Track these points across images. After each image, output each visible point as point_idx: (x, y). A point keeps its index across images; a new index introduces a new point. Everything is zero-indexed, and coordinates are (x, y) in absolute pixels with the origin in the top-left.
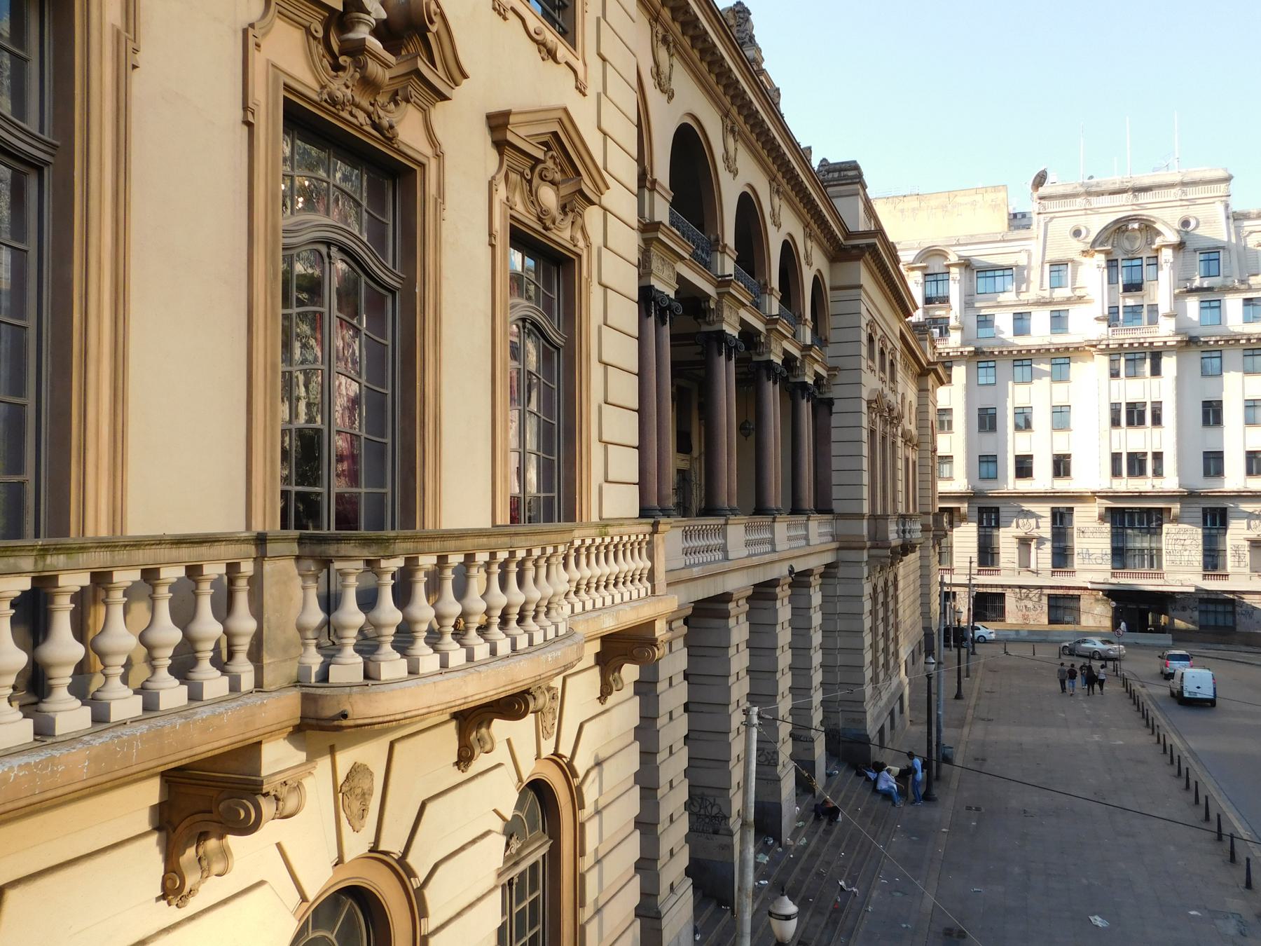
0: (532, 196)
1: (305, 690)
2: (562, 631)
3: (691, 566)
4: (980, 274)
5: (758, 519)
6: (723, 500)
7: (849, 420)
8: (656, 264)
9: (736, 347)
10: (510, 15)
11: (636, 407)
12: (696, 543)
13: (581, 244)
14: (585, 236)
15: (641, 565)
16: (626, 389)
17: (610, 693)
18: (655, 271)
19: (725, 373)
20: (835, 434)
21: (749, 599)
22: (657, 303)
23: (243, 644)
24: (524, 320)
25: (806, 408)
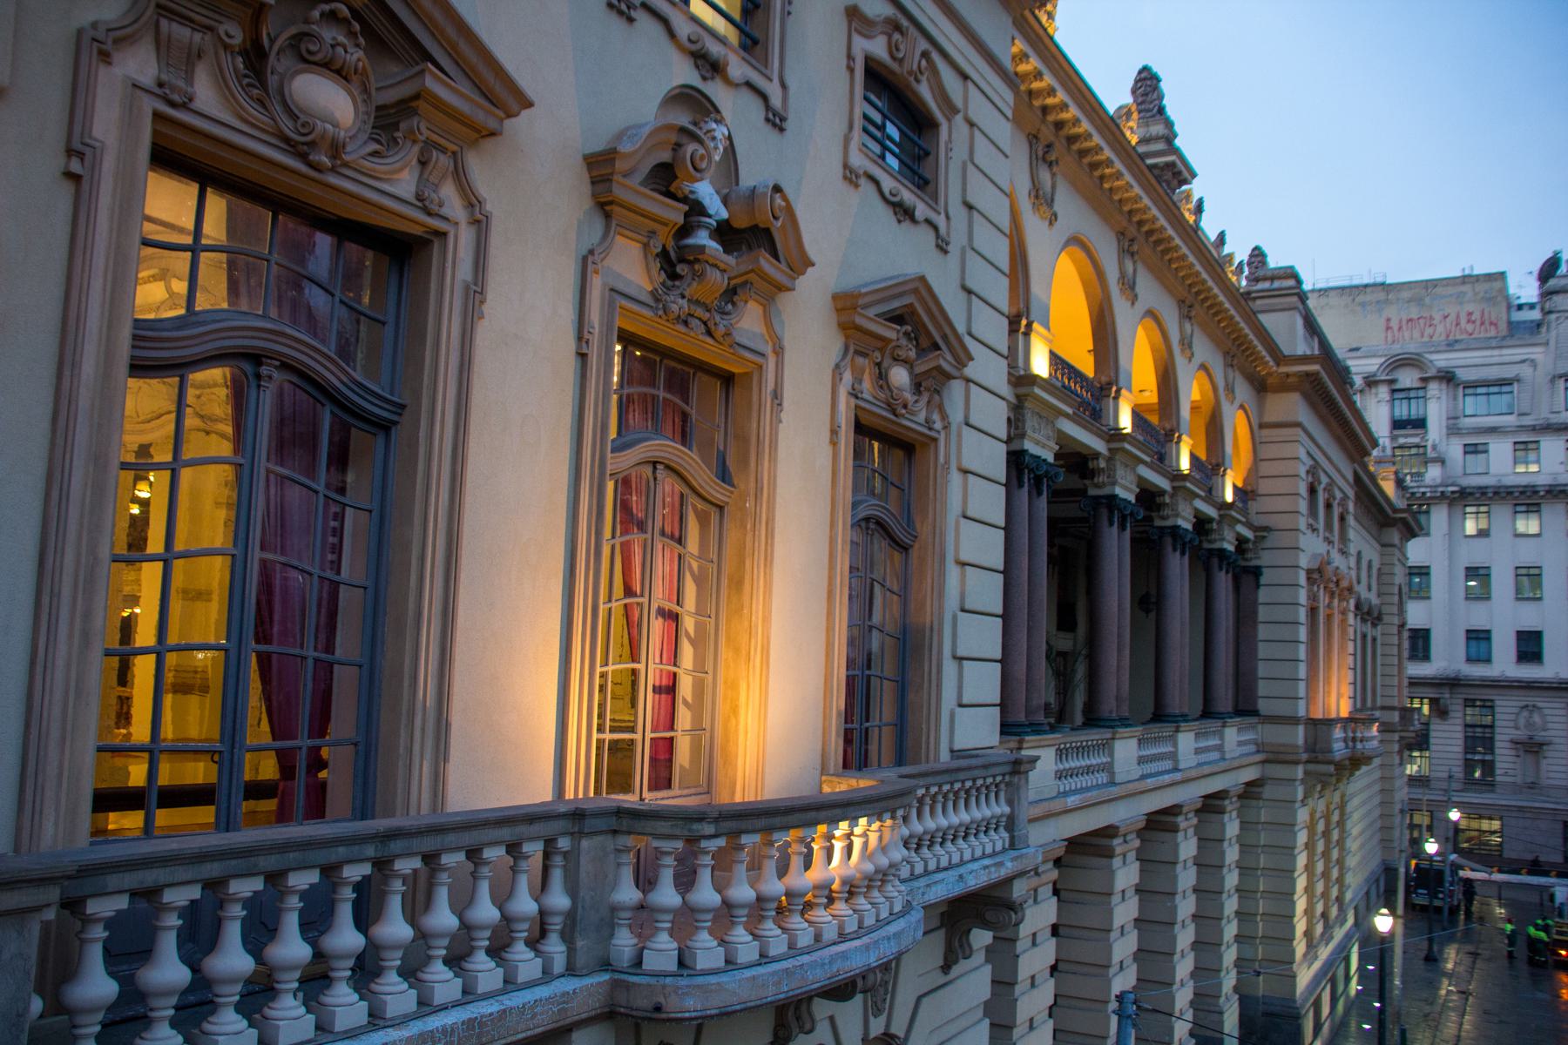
0: (882, 377)
1: (617, 976)
2: (897, 908)
3: (1066, 794)
4: (1469, 391)
5: (1156, 729)
6: (1108, 706)
7: (1284, 595)
8: (1030, 423)
9: (1131, 514)
10: (863, 181)
11: (1000, 611)
12: (1073, 763)
13: (938, 425)
14: (944, 417)
15: (998, 810)
16: (988, 592)
17: (956, 962)
18: (1029, 432)
19: (1116, 548)
20: (1263, 613)
21: (1140, 833)
22: (1031, 471)
23: (556, 923)
24: (867, 519)
25: (1223, 581)
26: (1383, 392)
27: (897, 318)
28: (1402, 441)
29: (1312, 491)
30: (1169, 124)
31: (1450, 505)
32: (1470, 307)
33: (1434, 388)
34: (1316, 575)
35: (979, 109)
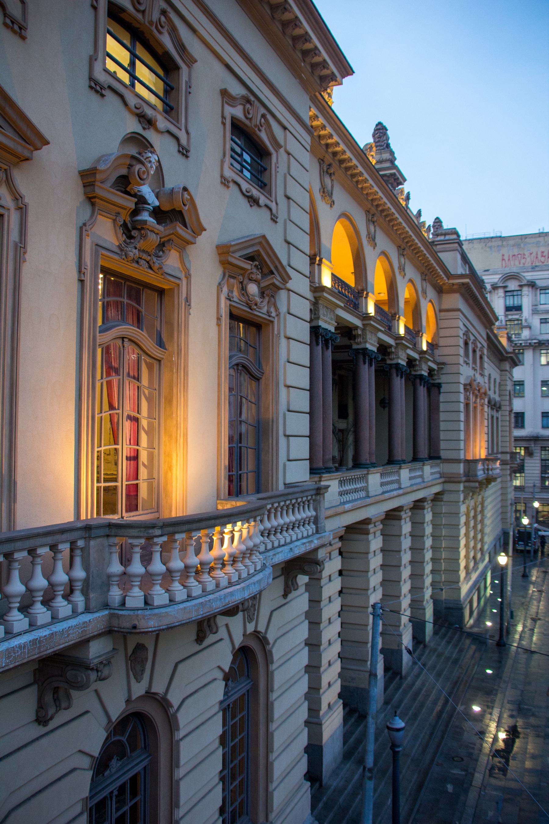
0: (243, 289)
1: (112, 611)
2: (258, 568)
3: (344, 503)
4: (542, 292)
5: (389, 468)
6: (365, 457)
7: (452, 397)
8: (322, 311)
9: (375, 358)
10: (231, 184)
11: (308, 410)
12: (348, 487)
13: (274, 314)
14: (277, 309)
15: (309, 514)
16: (302, 401)
17: (290, 592)
18: (321, 316)
19: (367, 375)
20: (442, 407)
21: (382, 521)
22: (323, 336)
23: (78, 585)
24: (237, 365)
25: (422, 391)
26: (501, 292)
27: (251, 258)
28: (510, 317)
29: (466, 344)
30: (392, 153)
31: (534, 350)
32: (542, 249)
33: (525, 290)
34: (468, 387)
35: (292, 146)
